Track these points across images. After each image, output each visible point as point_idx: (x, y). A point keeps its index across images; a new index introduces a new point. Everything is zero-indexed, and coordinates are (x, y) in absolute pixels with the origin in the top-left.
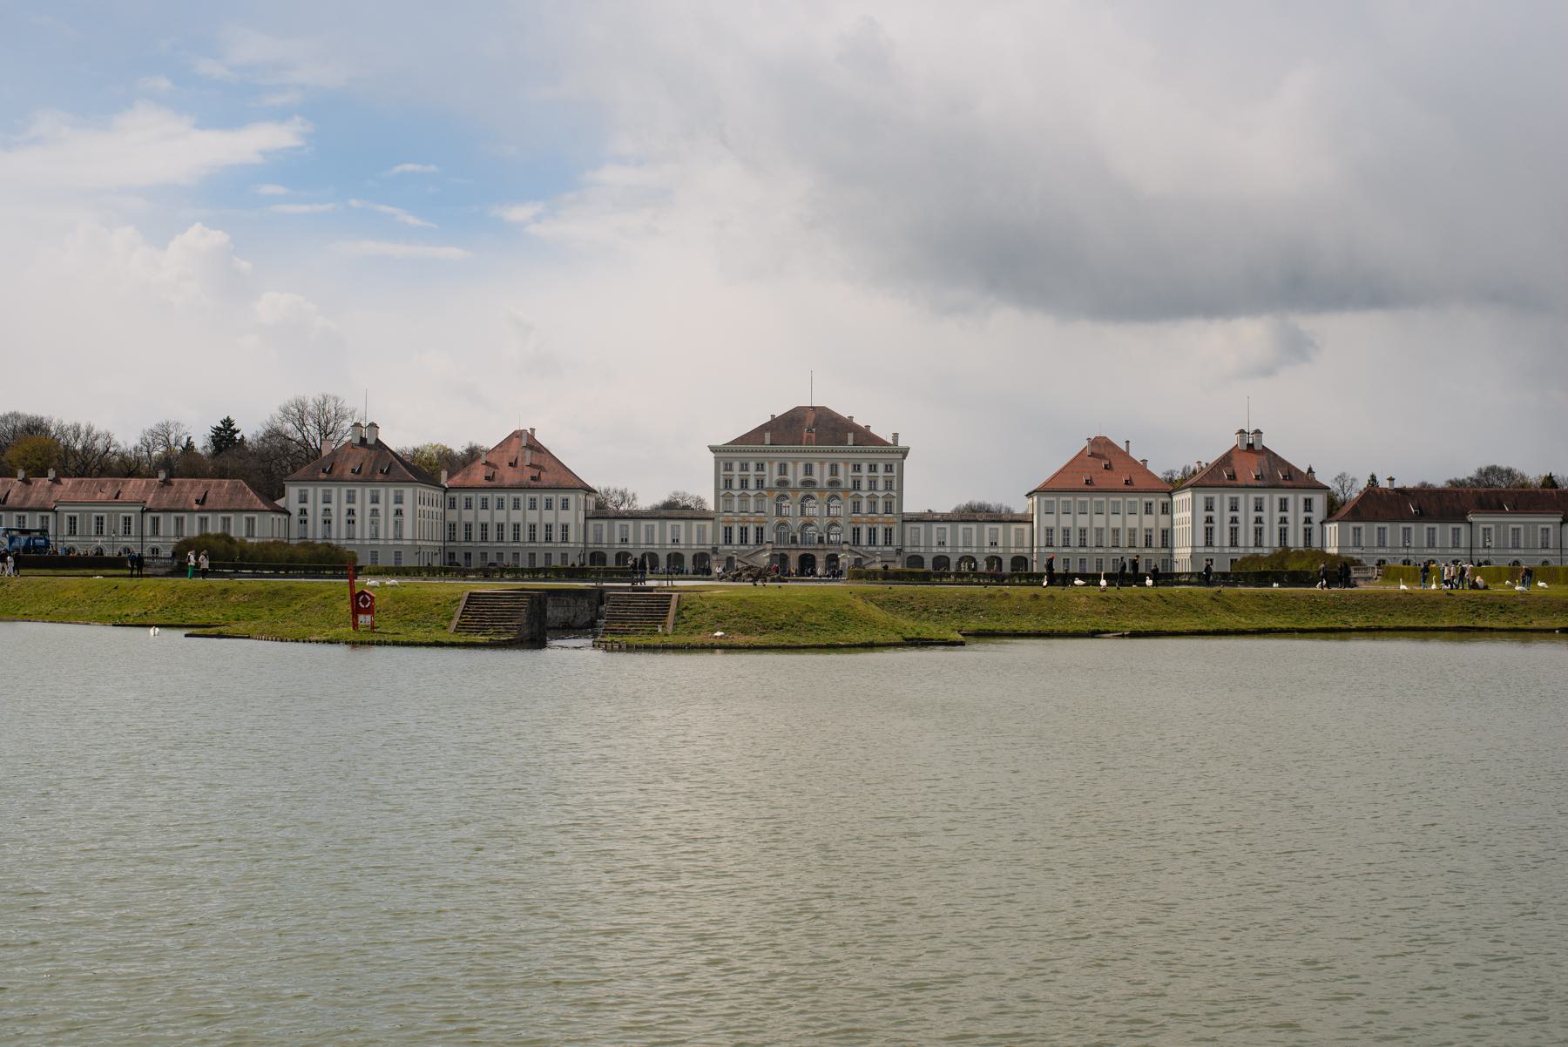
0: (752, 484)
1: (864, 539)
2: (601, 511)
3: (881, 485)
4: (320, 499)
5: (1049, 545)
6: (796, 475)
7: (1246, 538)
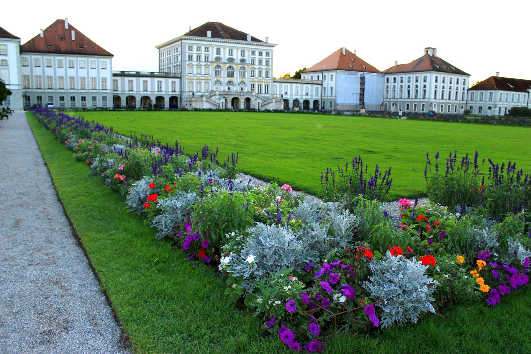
0: (203, 59)
3: (264, 63)
6: (225, 55)
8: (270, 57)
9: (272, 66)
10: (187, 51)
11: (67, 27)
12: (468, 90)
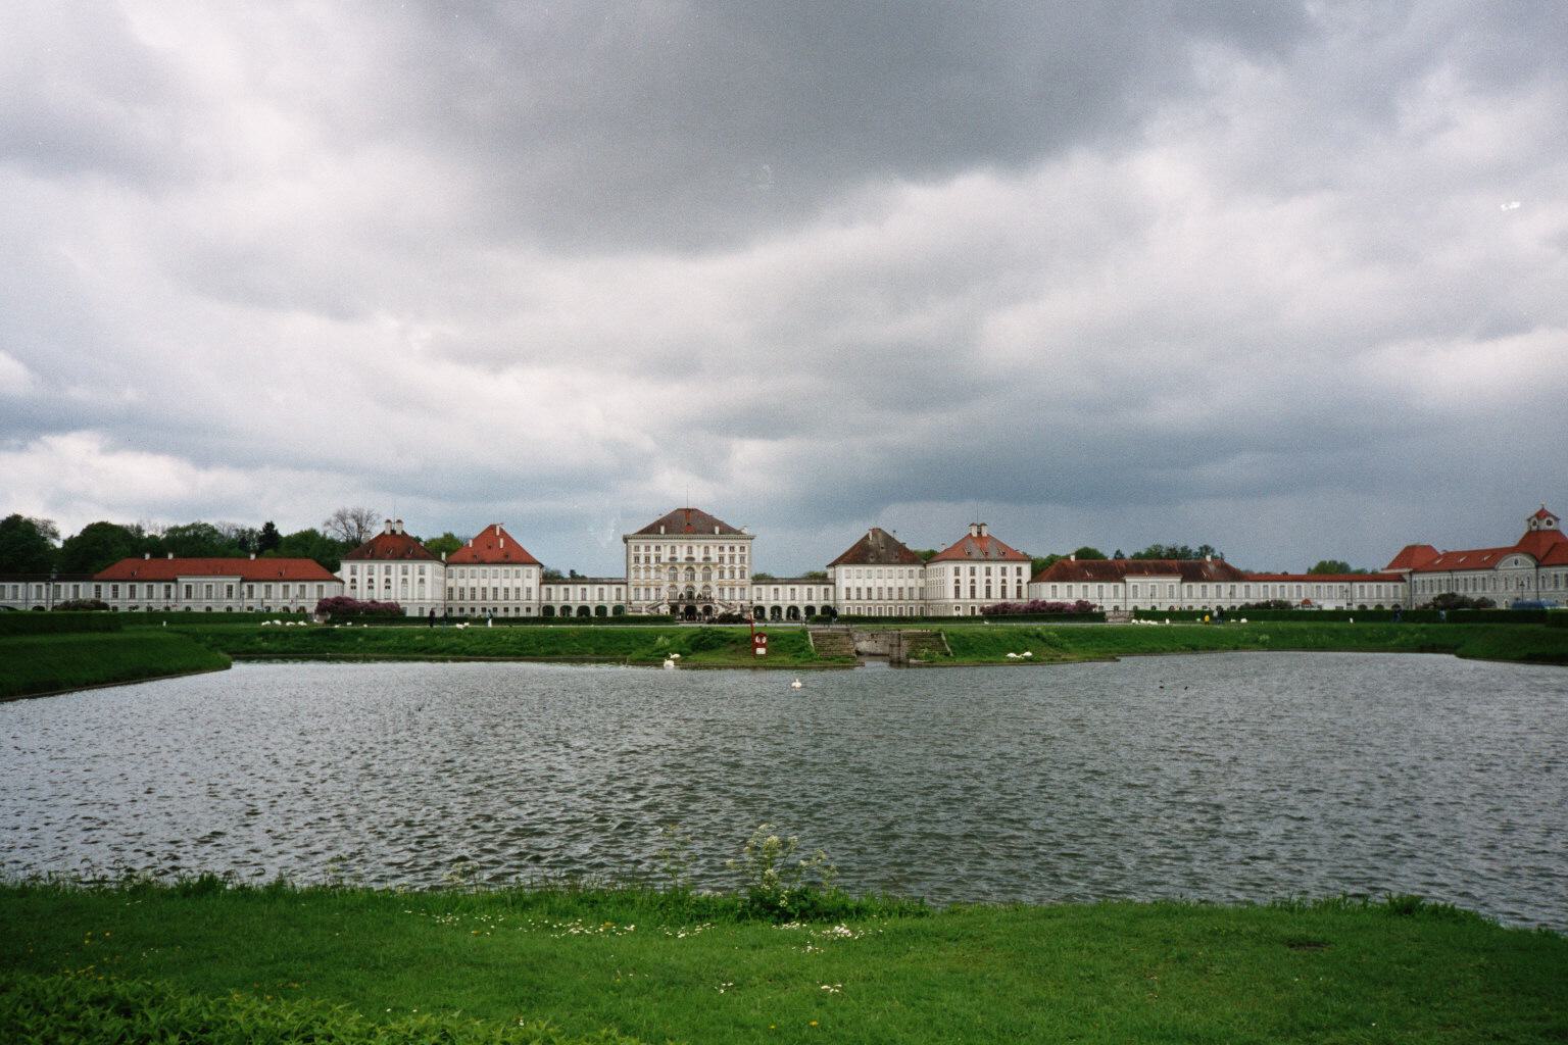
0: (653, 560)
1: (727, 597)
2: (550, 578)
3: (737, 560)
4: (366, 573)
5: (848, 598)
6: (682, 554)
7: (980, 592)
8: (747, 552)
11: (498, 533)
12: (1028, 583)
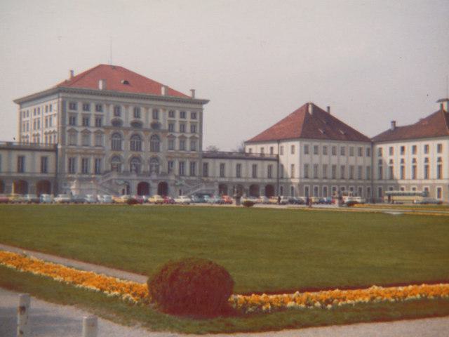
0: (92, 122)
3: (188, 128)
5: (306, 177)
6: (127, 117)
8: (198, 120)
9: (201, 136)
10: (68, 110)
